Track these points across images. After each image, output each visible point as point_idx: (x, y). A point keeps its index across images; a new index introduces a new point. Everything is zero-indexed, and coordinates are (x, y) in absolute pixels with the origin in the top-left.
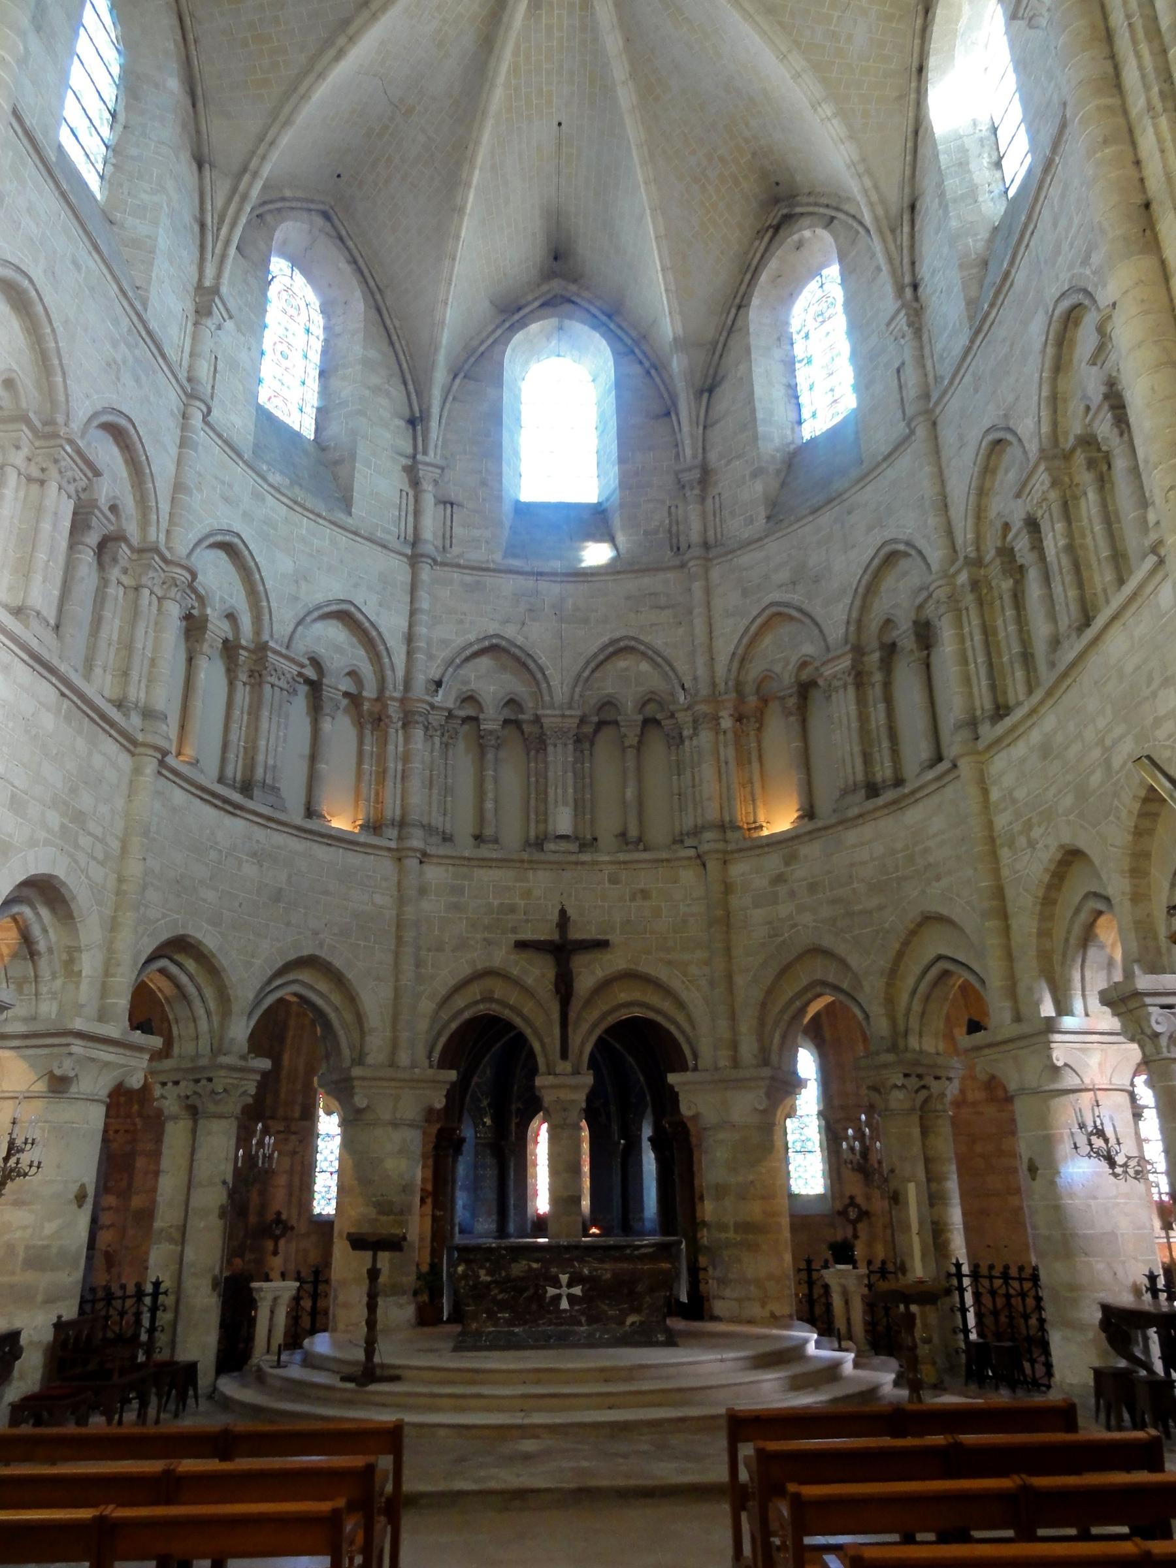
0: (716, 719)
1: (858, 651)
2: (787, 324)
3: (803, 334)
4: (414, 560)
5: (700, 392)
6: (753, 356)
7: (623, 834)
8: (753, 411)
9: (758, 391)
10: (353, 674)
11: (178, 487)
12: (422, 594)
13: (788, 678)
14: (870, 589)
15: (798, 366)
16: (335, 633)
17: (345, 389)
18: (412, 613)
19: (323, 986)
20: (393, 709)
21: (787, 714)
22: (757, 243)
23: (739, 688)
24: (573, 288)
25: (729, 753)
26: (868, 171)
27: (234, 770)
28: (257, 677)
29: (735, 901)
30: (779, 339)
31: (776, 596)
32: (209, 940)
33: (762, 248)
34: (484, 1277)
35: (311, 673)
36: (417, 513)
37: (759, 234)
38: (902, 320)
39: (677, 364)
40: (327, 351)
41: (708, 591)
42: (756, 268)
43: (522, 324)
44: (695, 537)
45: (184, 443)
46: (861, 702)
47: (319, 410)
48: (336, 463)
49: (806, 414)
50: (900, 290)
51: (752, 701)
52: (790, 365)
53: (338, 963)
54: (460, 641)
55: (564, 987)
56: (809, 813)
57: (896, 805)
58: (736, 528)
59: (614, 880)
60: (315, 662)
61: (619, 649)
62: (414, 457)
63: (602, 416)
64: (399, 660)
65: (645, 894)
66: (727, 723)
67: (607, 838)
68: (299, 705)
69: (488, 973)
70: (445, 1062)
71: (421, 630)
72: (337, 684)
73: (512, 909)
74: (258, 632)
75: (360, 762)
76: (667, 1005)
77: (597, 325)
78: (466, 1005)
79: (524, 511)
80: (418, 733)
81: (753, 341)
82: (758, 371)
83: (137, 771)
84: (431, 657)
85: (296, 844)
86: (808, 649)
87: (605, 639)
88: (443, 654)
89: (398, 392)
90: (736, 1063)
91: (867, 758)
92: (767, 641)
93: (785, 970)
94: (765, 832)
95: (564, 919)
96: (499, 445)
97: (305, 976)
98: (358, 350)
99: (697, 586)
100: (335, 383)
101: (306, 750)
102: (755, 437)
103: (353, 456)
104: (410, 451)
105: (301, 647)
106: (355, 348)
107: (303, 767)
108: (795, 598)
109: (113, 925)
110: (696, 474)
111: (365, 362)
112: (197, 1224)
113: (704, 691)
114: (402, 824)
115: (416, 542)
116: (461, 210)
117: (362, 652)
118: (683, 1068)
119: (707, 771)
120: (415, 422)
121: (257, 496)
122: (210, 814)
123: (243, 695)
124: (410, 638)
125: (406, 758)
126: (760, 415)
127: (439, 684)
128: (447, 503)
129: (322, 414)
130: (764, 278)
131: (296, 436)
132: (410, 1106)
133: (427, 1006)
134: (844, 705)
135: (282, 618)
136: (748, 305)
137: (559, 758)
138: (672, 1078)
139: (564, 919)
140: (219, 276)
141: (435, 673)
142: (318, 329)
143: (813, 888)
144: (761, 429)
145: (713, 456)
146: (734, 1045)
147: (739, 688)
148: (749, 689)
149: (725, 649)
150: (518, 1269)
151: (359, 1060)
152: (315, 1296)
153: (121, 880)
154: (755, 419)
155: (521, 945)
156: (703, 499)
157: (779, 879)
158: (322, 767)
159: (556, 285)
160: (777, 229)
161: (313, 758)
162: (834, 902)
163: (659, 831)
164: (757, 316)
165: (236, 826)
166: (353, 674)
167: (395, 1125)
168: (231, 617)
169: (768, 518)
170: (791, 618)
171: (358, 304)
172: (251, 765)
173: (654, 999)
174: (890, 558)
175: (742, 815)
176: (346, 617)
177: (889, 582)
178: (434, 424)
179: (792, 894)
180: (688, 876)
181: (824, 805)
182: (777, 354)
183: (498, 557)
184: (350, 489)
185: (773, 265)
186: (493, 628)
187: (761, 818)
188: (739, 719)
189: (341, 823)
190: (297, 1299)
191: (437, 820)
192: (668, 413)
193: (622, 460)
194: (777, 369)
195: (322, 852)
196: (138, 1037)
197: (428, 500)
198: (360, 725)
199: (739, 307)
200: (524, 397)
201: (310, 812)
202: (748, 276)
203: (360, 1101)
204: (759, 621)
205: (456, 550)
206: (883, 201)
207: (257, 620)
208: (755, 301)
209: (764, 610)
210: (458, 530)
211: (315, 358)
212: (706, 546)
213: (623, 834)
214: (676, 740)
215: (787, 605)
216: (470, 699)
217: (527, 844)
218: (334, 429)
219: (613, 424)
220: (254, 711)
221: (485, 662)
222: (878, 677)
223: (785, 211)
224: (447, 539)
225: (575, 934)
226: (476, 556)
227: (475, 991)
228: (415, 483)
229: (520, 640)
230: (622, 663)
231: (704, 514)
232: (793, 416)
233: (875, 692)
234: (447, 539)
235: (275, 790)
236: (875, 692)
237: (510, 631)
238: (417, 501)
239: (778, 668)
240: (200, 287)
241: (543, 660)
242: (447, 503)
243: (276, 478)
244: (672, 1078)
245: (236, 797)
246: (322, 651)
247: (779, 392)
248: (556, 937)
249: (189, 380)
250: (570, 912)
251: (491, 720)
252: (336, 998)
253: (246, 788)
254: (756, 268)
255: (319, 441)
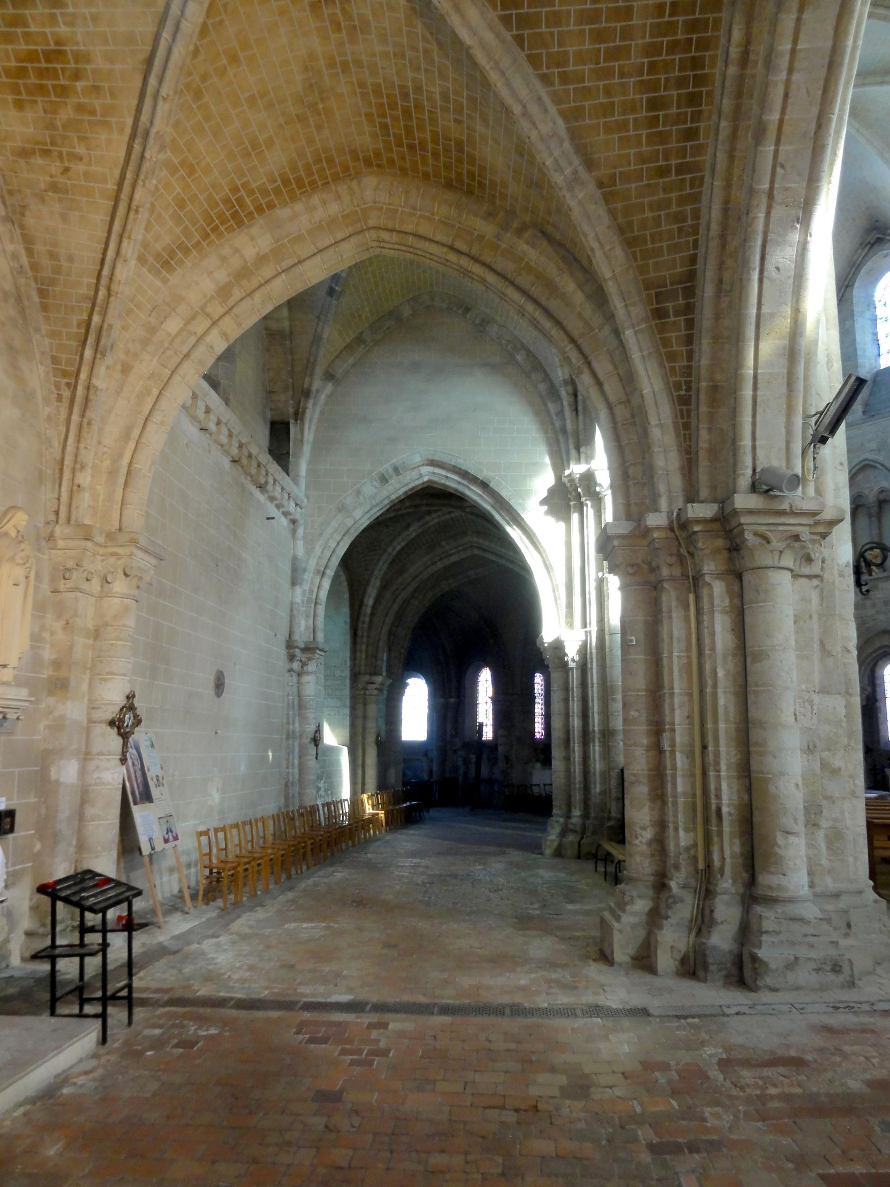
2: (873, 296)
3: (882, 302)
6: (856, 317)
8: (855, 350)
15: (878, 321)
21: (870, 516)
22: (860, 251)
30: (868, 305)
31: (868, 455)
33: (863, 254)
42: (859, 265)
49: (883, 350)
52: (874, 320)
108: (880, 458)
126: (859, 353)
130: (863, 271)
136: (853, 285)
144: (860, 361)
154: (856, 355)
160: (873, 245)
169: (864, 412)
170: (876, 467)
179: (874, 605)
182: (868, 314)
185: (869, 264)
199: (847, 287)
202: (854, 270)
204: (858, 467)
208: (857, 284)
209: (861, 462)
215: (875, 462)
223: (880, 236)
232: (876, 352)
239: (866, 492)
247: (869, 338)
254: (859, 265)
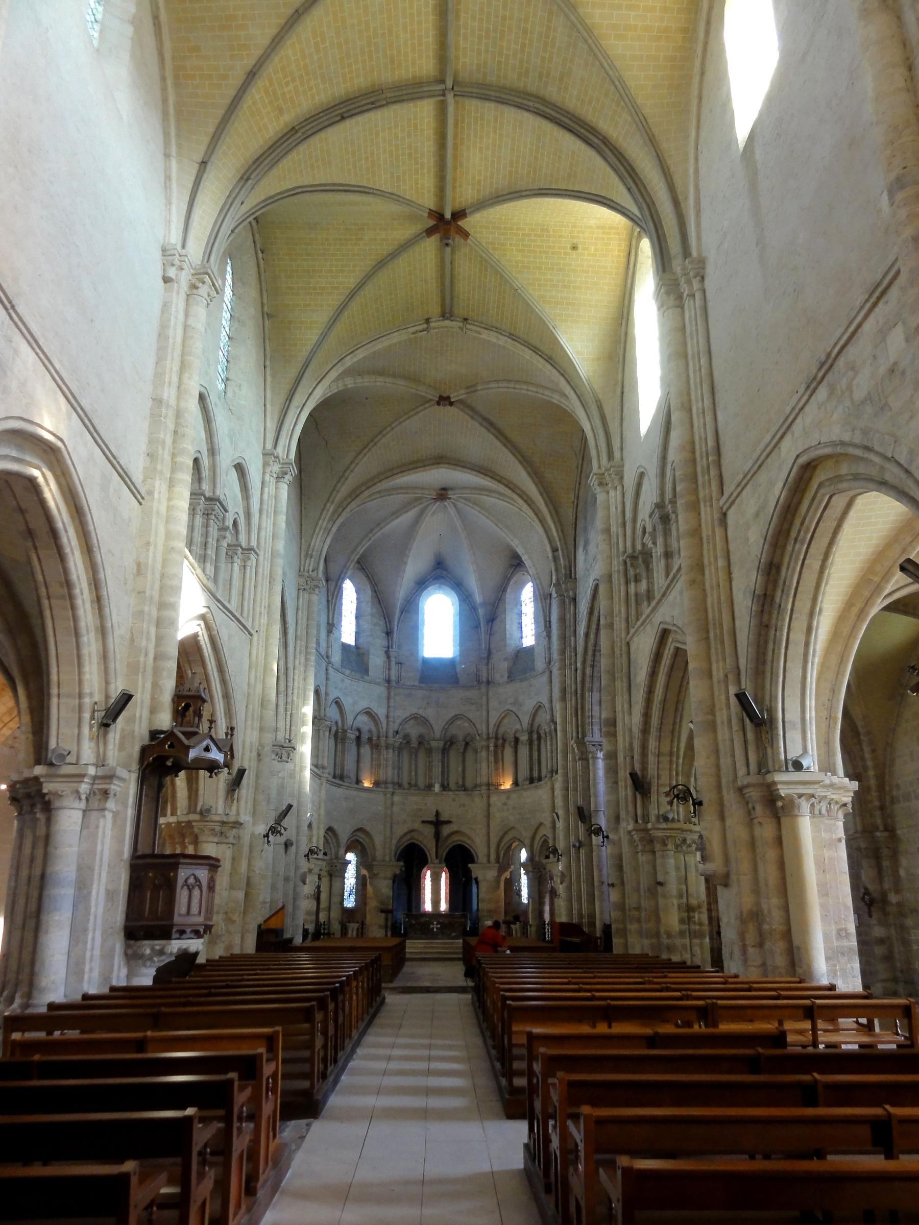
0: (488, 747)
1: (530, 733)
4: (389, 688)
5: (488, 622)
7: (457, 783)
9: (507, 627)
10: (370, 731)
11: (327, 694)
12: (392, 701)
13: (512, 736)
14: (534, 715)
16: (364, 718)
17: (366, 626)
18: (388, 707)
19: (363, 836)
20: (383, 743)
23: (497, 734)
24: (445, 573)
25: (492, 759)
26: (539, 578)
27: (338, 772)
28: (344, 740)
29: (492, 810)
32: (335, 827)
34: (413, 922)
35: (357, 734)
36: (389, 669)
37: (512, 566)
38: (545, 633)
39: (481, 611)
40: (357, 609)
41: (488, 700)
43: (426, 588)
44: (484, 679)
45: (327, 679)
46: (531, 750)
47: (356, 633)
48: (363, 654)
50: (545, 621)
51: (500, 741)
52: (520, 614)
53: (368, 829)
54: (404, 716)
55: (437, 835)
56: (516, 783)
57: (536, 787)
58: (497, 677)
59: (454, 800)
60: (359, 730)
61: (456, 717)
62: (388, 648)
63: (455, 621)
64: (384, 725)
65: (464, 806)
66: (492, 748)
67: (452, 785)
68: (354, 747)
69: (413, 831)
70: (398, 860)
71: (391, 714)
72: (365, 737)
73: (421, 810)
74: (343, 725)
75: (372, 761)
76: (469, 842)
77: (453, 588)
78: (405, 842)
79: (425, 661)
80: (391, 751)
81: (508, 607)
82: (508, 621)
83: (321, 784)
84: (394, 722)
85: (355, 793)
86: (518, 727)
87: (453, 714)
88: (398, 721)
89: (382, 623)
90: (489, 862)
91: (531, 770)
92: (506, 721)
93: (506, 833)
94: (502, 788)
95: (438, 814)
96: (417, 639)
97: (358, 834)
98: (369, 609)
99: (484, 698)
100: (361, 622)
101: (356, 759)
102: (505, 645)
103: (368, 654)
104: (386, 645)
105: (354, 727)
106: (368, 609)
107: (355, 765)
109: (318, 828)
110: (485, 655)
111: (372, 615)
112: (333, 907)
113: (485, 737)
114: (386, 783)
115: (388, 681)
116: (406, 564)
117: (372, 723)
118: (473, 861)
119: (484, 765)
120: (389, 633)
121: (343, 681)
122: (335, 789)
123: (339, 746)
124: (387, 717)
125: (387, 760)
127: (397, 732)
128: (399, 663)
129: (358, 634)
131: (349, 646)
132: (389, 873)
133: (394, 842)
134: (524, 751)
135: (350, 718)
137: (437, 758)
138: (470, 865)
139: (438, 814)
140: (333, 618)
141: (396, 728)
142: (355, 601)
143: (514, 808)
144: (508, 642)
145: (492, 647)
146: (489, 856)
147: (497, 734)
148: (500, 736)
149: (493, 721)
150: (422, 920)
151: (374, 859)
152: (362, 928)
153: (319, 816)
155: (423, 822)
156: (488, 664)
157: (505, 804)
158: (361, 765)
159: (439, 572)
161: (358, 761)
162: (520, 814)
163: (469, 784)
164: (509, 595)
165: (340, 790)
166: (370, 731)
167: (385, 878)
168: (336, 723)
171: (369, 592)
172: (342, 769)
173: (465, 839)
174: (539, 707)
175: (494, 780)
176: (368, 713)
177: (540, 713)
178: (395, 635)
180: (477, 800)
181: (520, 780)
182: (516, 611)
183: (417, 684)
184: (368, 665)
186: (415, 711)
187: (501, 782)
188: (496, 746)
189: (367, 784)
190: (358, 929)
191: (396, 781)
192: (477, 627)
193: (461, 644)
194: (515, 617)
195: (363, 795)
196: (325, 857)
197: (393, 663)
198: (372, 749)
200: (426, 637)
201: (358, 781)
203: (375, 872)
205: (402, 682)
206: (543, 588)
207: (343, 721)
208: (509, 590)
210: (403, 674)
211: (354, 612)
212: (488, 683)
213: (457, 783)
214: (476, 751)
216: (406, 737)
217: (426, 786)
218: (361, 641)
219: (458, 628)
220: (343, 752)
221: (412, 722)
222: (536, 742)
224: (399, 678)
225: (442, 819)
226: (410, 683)
227: (409, 836)
228: (388, 657)
229: (424, 715)
230: (459, 722)
231: (488, 670)
232: (519, 636)
233: (535, 747)
234: (399, 678)
235: (349, 777)
236: (535, 747)
237: (421, 712)
238: (389, 665)
240: (328, 623)
241: (432, 722)
242: (399, 663)
243: (347, 672)
244: (470, 865)
245: (341, 783)
246: (361, 726)
247: (515, 626)
248: (434, 819)
249: (327, 657)
250: (440, 810)
251: (414, 744)
252: (367, 840)
253: (341, 777)
255: (357, 646)
